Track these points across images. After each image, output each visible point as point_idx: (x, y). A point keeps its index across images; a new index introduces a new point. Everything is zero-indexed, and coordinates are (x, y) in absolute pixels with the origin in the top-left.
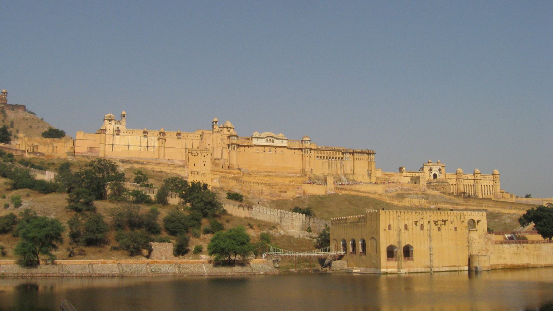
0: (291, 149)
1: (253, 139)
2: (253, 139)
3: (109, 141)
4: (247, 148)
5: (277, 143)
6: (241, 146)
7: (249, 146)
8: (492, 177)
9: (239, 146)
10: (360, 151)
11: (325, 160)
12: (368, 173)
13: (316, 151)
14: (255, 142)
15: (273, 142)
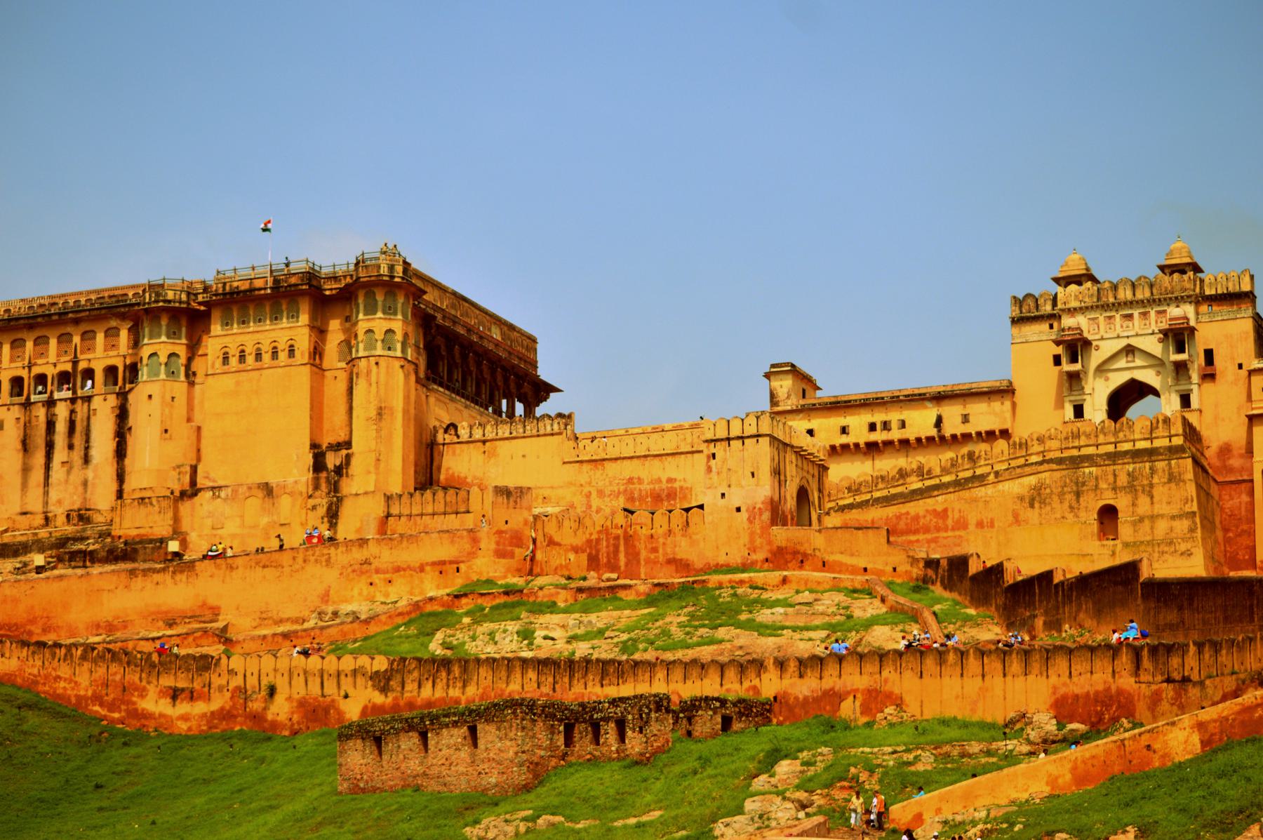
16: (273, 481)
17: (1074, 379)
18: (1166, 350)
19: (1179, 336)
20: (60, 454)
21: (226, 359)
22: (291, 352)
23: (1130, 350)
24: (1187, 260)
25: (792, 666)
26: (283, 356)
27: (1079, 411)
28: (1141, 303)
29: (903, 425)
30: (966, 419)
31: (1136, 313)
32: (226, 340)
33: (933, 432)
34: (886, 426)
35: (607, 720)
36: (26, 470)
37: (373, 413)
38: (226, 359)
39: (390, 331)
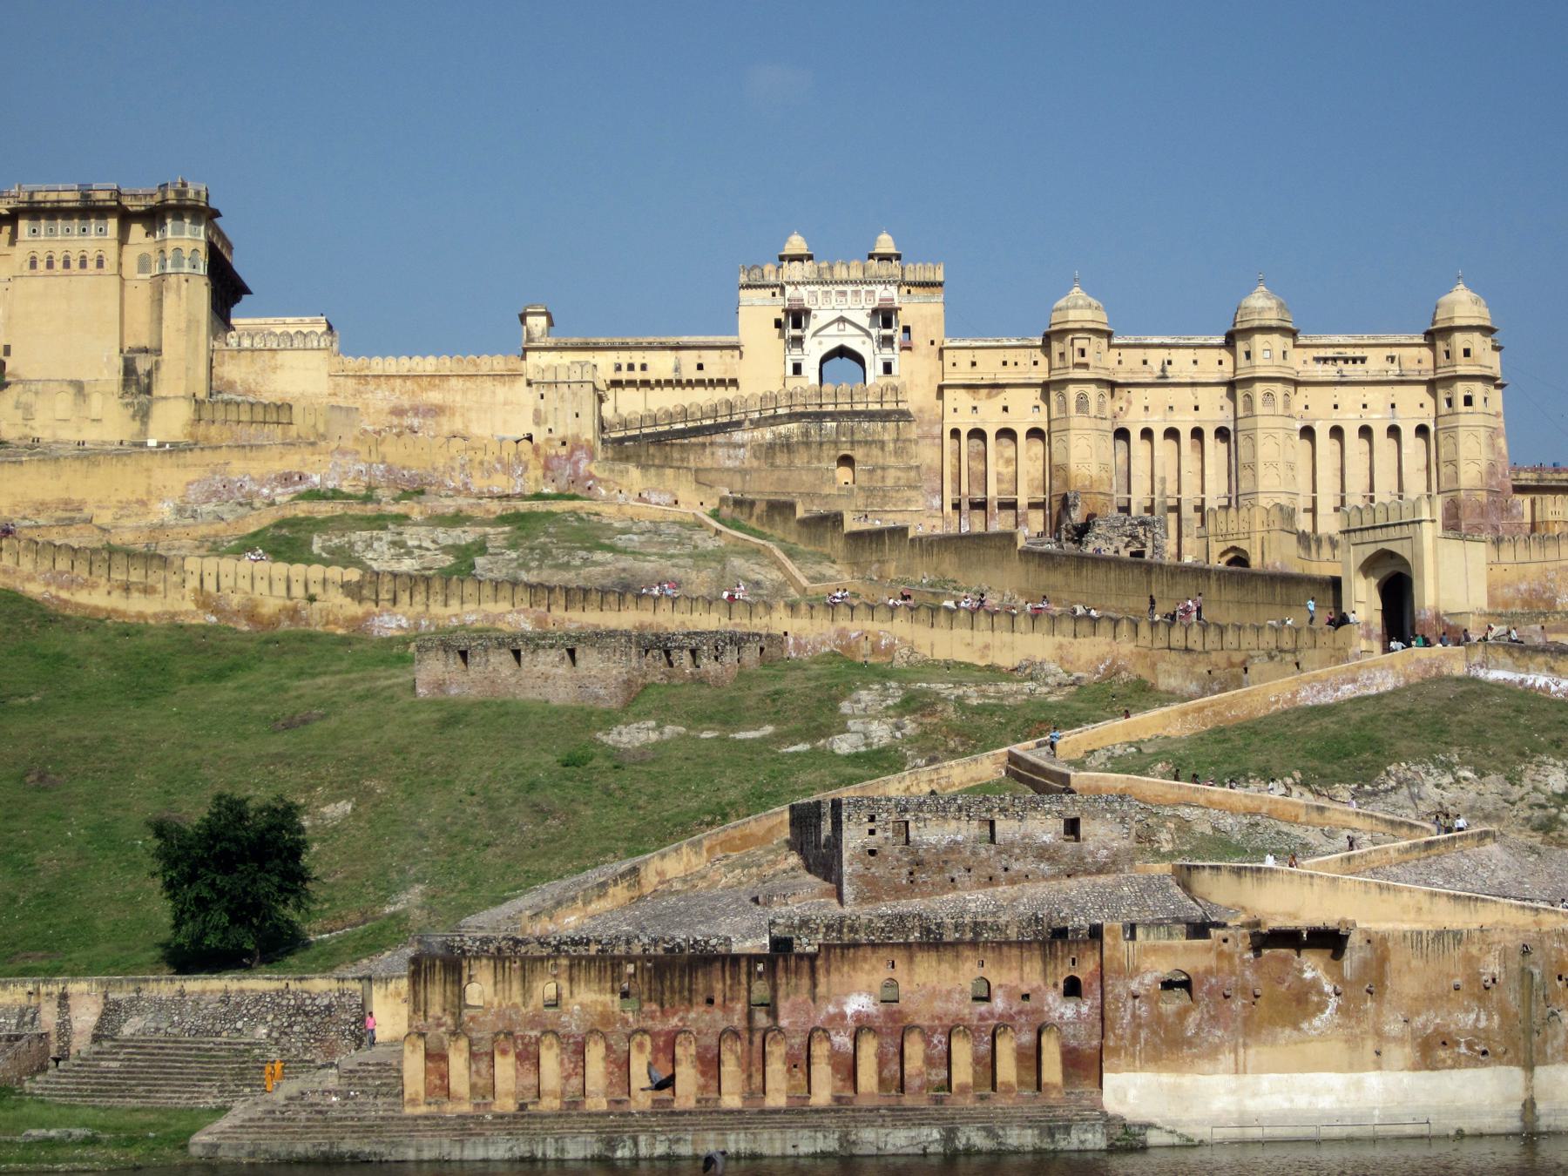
8: (1418, 359)
10: (70, 197)
12: (129, 370)
16: (84, 377)
17: (798, 341)
18: (872, 325)
19: (885, 315)
21: (33, 264)
22: (100, 264)
23: (842, 320)
24: (892, 250)
25: (804, 608)
26: (91, 265)
27: (797, 369)
28: (855, 282)
29: (644, 367)
30: (700, 367)
31: (849, 289)
32: (34, 246)
33: (671, 376)
34: (631, 367)
35: (681, 648)
37: (183, 325)
38: (33, 264)
39: (195, 250)
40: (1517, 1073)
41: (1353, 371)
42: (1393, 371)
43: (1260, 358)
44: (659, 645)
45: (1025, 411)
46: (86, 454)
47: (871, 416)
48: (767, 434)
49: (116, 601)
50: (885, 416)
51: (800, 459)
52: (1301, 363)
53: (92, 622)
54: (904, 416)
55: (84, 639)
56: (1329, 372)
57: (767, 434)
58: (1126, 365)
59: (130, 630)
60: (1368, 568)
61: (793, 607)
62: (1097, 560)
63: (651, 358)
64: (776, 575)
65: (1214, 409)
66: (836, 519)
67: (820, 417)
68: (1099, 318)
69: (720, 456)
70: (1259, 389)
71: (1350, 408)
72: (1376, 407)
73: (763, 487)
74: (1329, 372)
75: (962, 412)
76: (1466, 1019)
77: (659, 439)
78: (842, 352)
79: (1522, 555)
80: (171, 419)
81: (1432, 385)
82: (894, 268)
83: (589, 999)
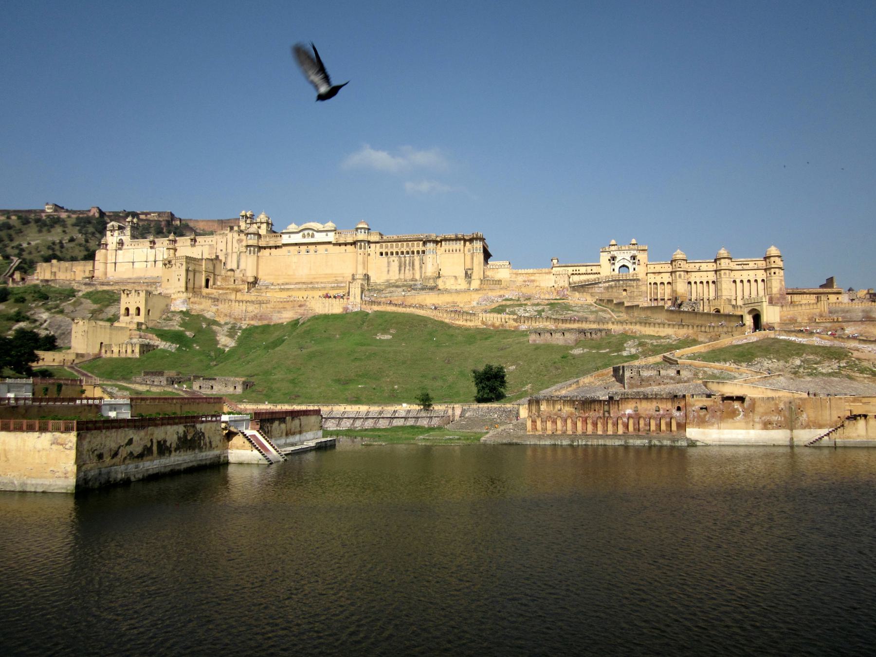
0: (340, 245)
1: (283, 236)
2: (283, 236)
3: (111, 259)
4: (273, 250)
5: (319, 237)
6: (265, 248)
7: (276, 247)
8: (762, 264)
9: (260, 248)
10: (453, 237)
11: (395, 258)
12: (466, 273)
13: (378, 245)
14: (285, 239)
15: (313, 236)
17: (614, 264)
19: (634, 257)
20: (407, 268)
36: (400, 270)
40: (788, 431)
41: (745, 267)
42: (756, 267)
43: (723, 265)
44: (583, 332)
45: (666, 278)
46: (458, 292)
47: (631, 280)
48: (607, 285)
49: (464, 323)
50: (634, 280)
51: (614, 290)
52: (733, 265)
53: (459, 327)
54: (638, 280)
55: (457, 331)
56: (740, 267)
57: (607, 285)
58: (691, 267)
59: (468, 329)
60: (750, 312)
61: (613, 323)
62: (684, 312)
63: (580, 268)
64: (609, 316)
65: (712, 277)
66: (623, 303)
67: (619, 280)
68: (684, 257)
69: (597, 290)
70: (723, 272)
71: (745, 276)
72: (751, 275)
73: (606, 296)
74: (740, 267)
75: (652, 279)
76: (775, 418)
77: (582, 286)
78: (624, 266)
79: (788, 309)
80: (475, 284)
81: (765, 270)
82: (636, 247)
83: (568, 409)
